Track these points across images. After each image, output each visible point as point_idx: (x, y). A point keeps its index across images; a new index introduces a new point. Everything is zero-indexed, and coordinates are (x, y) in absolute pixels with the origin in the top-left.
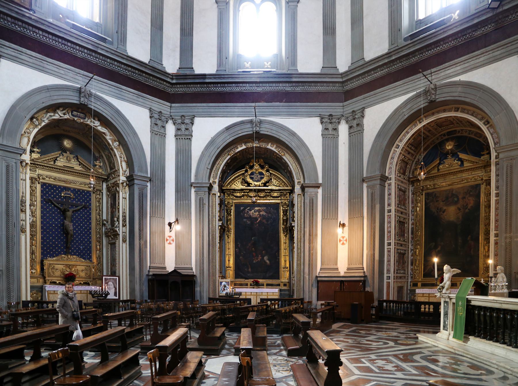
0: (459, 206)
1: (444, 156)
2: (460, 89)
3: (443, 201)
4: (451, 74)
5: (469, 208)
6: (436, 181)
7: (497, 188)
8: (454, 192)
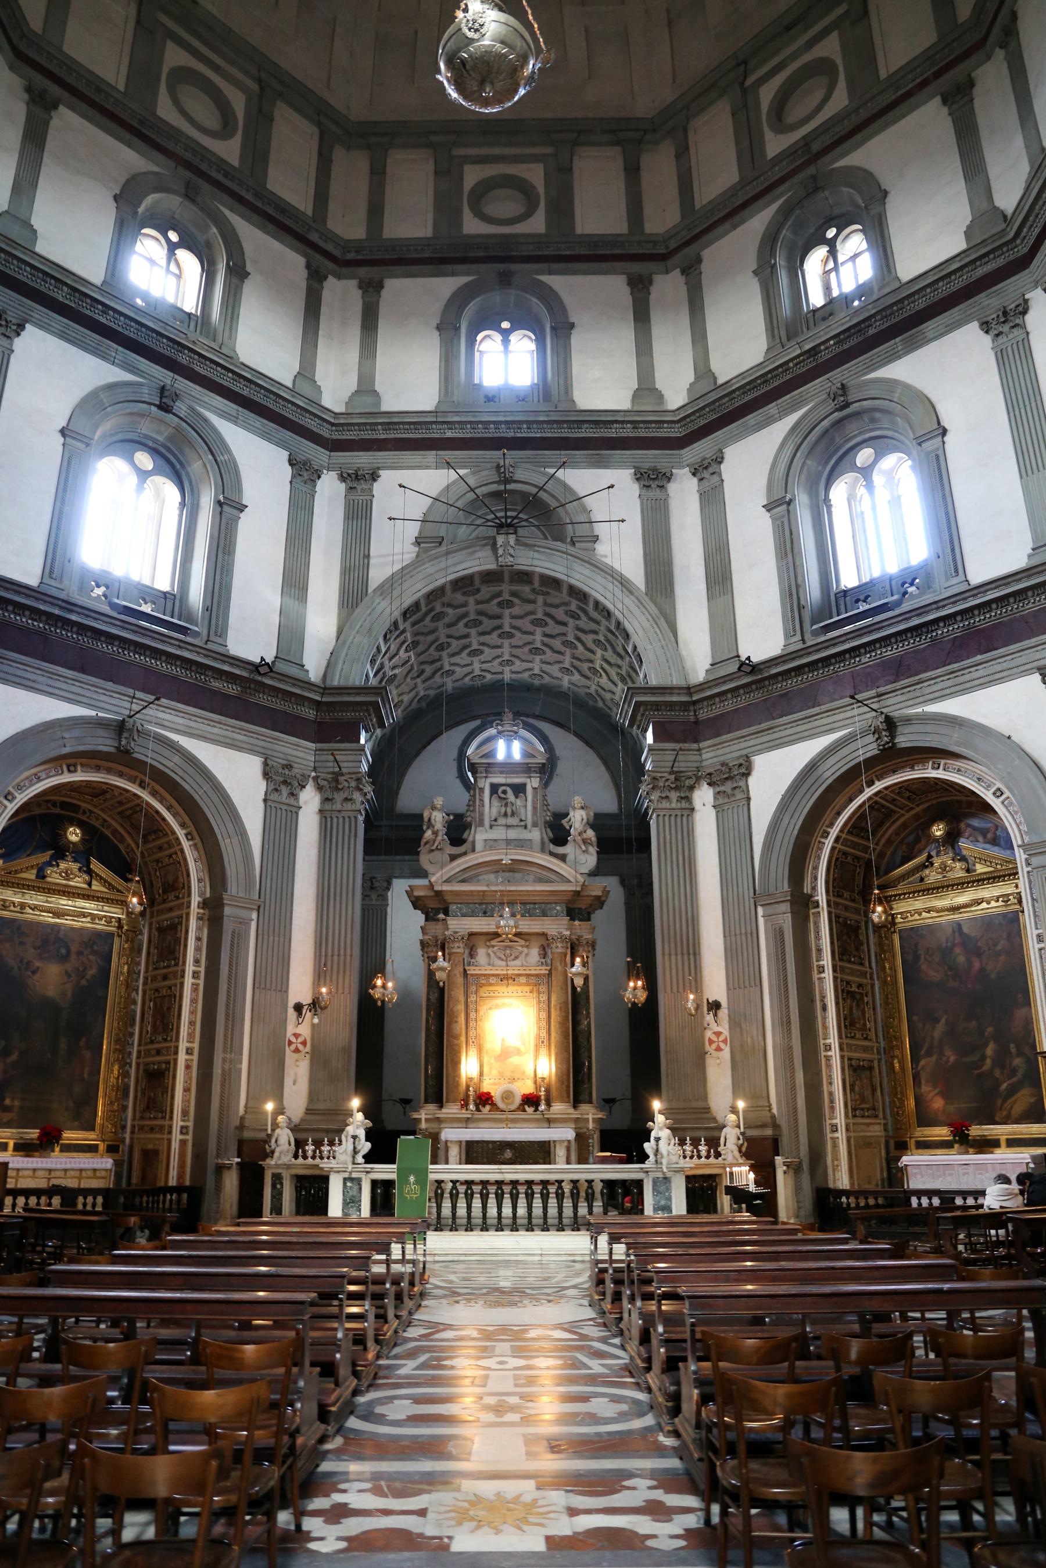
0: (68, 967)
1: (60, 851)
2: (176, 759)
3: (35, 948)
4: (166, 723)
5: (88, 977)
6: (27, 896)
7: (197, 962)
8: (61, 935)
